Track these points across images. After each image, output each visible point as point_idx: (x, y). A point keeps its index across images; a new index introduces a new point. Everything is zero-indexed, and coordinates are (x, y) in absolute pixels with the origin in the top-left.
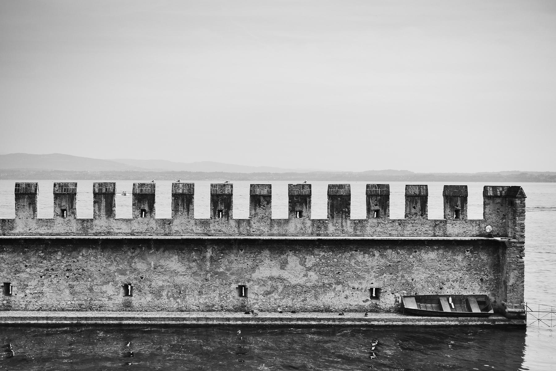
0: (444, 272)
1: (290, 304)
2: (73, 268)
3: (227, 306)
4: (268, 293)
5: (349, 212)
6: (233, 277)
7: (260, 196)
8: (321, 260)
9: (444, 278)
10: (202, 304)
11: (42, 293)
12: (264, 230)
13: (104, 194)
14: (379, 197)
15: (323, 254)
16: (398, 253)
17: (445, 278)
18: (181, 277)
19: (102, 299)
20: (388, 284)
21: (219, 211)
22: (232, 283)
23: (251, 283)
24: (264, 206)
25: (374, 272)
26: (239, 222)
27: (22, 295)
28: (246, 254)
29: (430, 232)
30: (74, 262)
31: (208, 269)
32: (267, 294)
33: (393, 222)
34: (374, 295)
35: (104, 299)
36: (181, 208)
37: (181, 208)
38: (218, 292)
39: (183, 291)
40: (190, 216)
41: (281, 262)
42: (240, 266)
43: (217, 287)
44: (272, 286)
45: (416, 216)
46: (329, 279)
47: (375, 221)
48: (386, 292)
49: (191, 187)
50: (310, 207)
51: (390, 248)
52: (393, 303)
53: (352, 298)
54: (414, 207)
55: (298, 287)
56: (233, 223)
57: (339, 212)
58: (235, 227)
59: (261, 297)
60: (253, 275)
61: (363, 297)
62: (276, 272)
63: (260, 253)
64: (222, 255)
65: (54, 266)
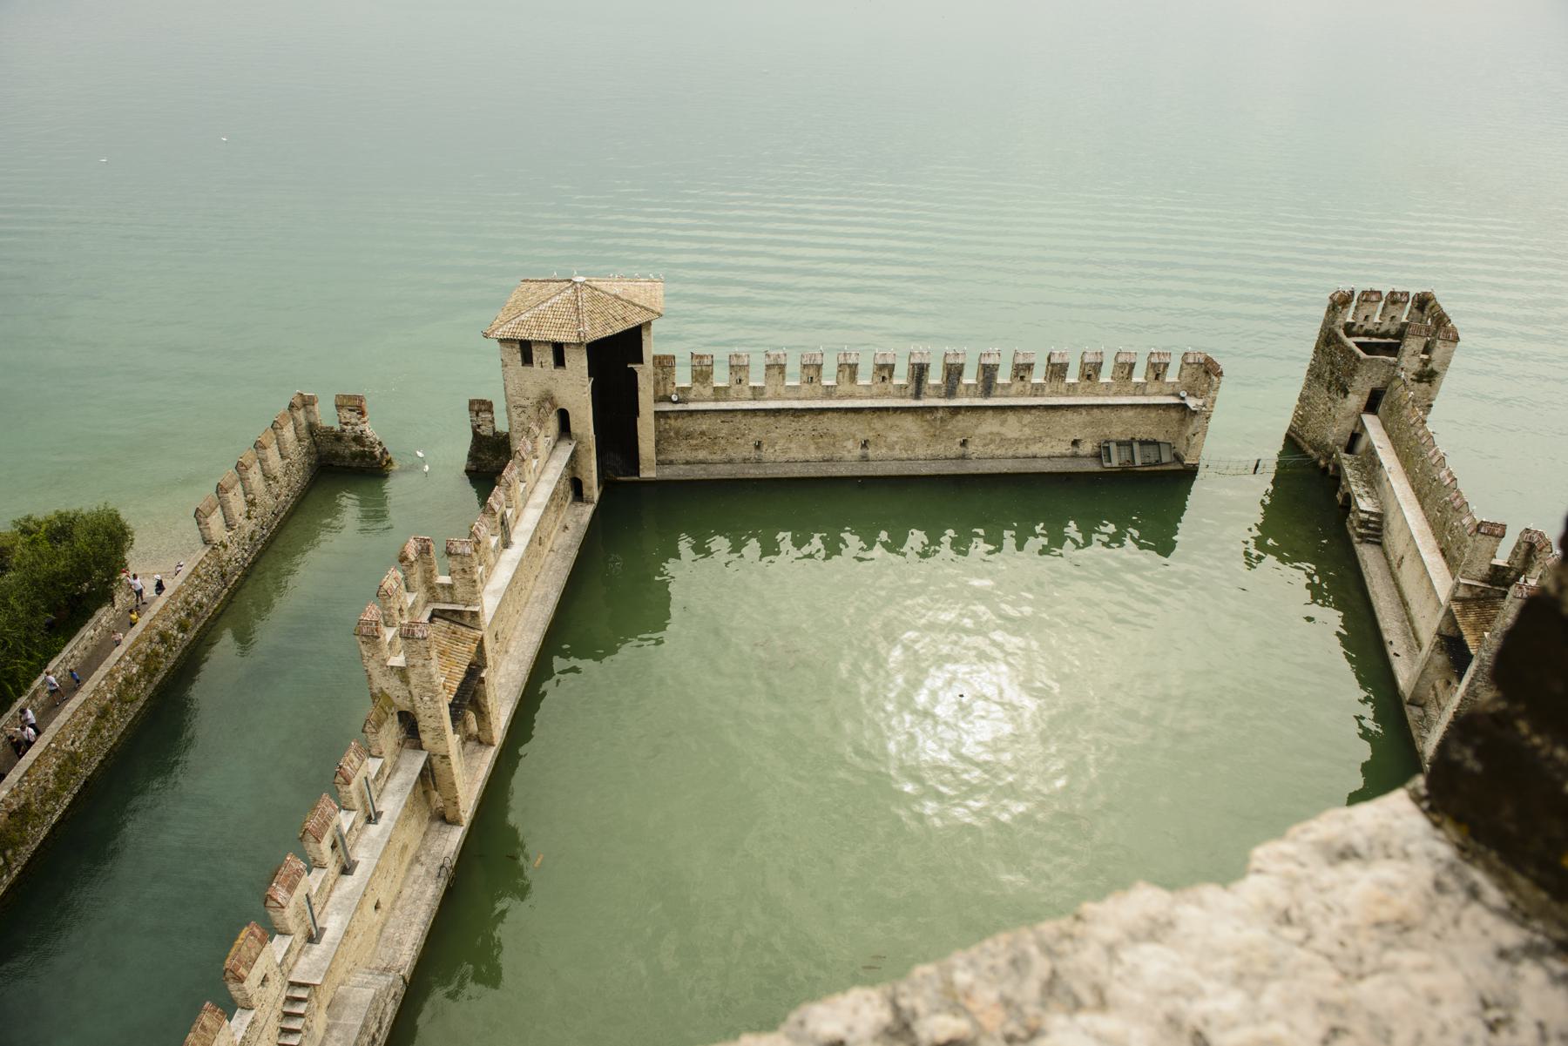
5: (1065, 377)
6: (958, 433)
11: (790, 449)
27: (772, 451)
42: (966, 424)
44: (991, 440)
59: (981, 448)
62: (996, 429)
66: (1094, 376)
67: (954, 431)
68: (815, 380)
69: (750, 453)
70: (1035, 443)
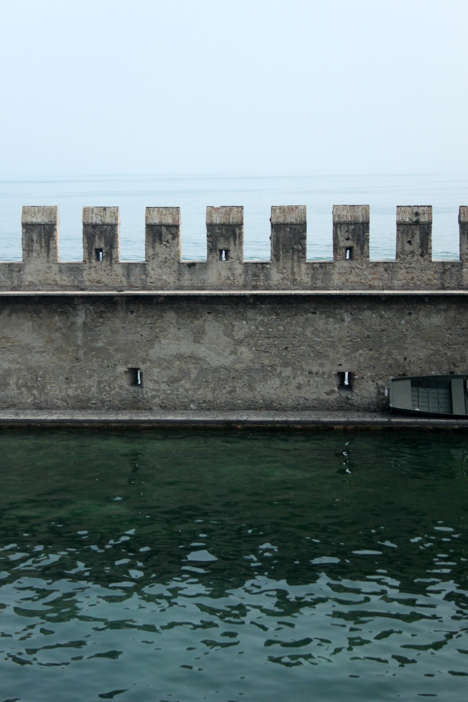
0: (455, 346)
1: (210, 396)
3: (110, 401)
4: (173, 381)
5: (304, 251)
6: (119, 356)
7: (161, 225)
8: (257, 328)
9: (456, 356)
10: (72, 397)
12: (169, 280)
14: (353, 227)
15: (262, 317)
16: (381, 317)
17: (458, 357)
18: (38, 355)
20: (365, 365)
21: (98, 251)
22: (117, 365)
23: (148, 364)
24: (167, 242)
25: (343, 347)
26: (129, 267)
28: (139, 319)
29: (435, 282)
31: (79, 342)
32: (173, 382)
33: (376, 266)
34: (346, 383)
36: (36, 246)
37: (36, 246)
38: (97, 379)
39: (41, 377)
40: (52, 258)
41: (195, 330)
42: (130, 337)
43: (95, 371)
44: (181, 370)
45: (413, 256)
46: (271, 358)
47: (345, 264)
48: (363, 378)
49: (52, 211)
50: (241, 243)
51: (369, 308)
52: (374, 395)
53: (308, 388)
54: (410, 242)
55: (222, 370)
56: (119, 270)
57: (287, 251)
58: (123, 275)
60: (151, 352)
61: (326, 387)
63: (161, 317)
64: (101, 320)
66: (357, 249)
67: (111, 349)
70: (264, 379)
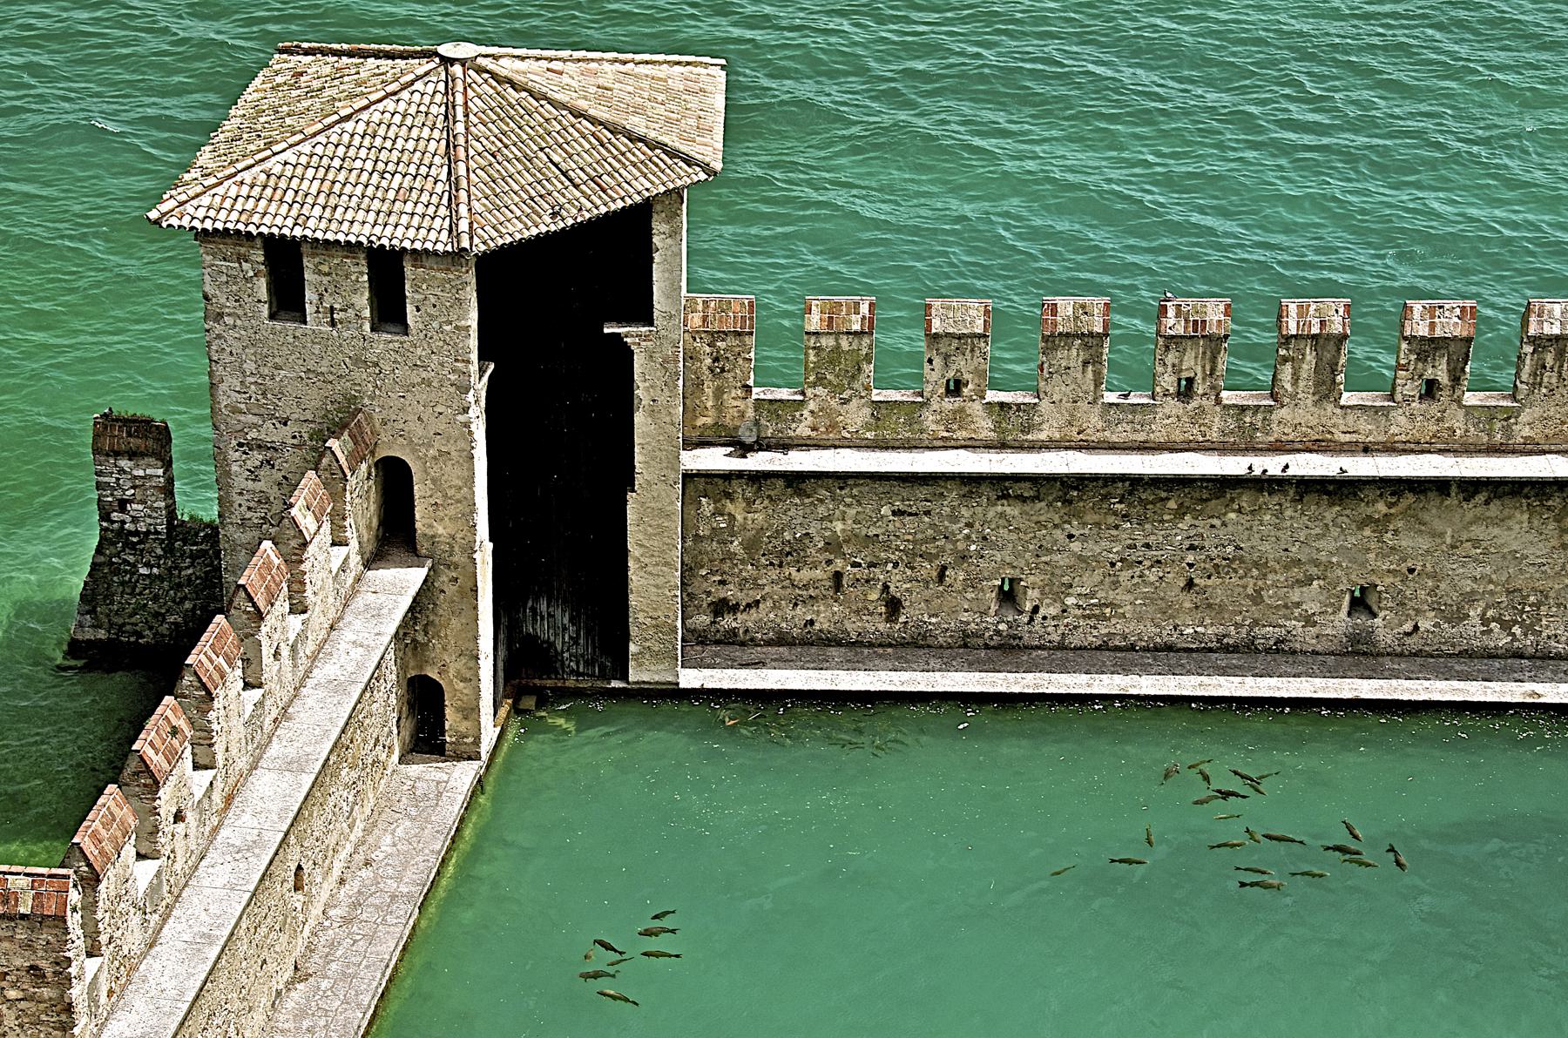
2: (1206, 544)
13: (1314, 337)
19: (1287, 624)
30: (1213, 526)
35: (1294, 622)
65: (1153, 537)
68: (1200, 388)
69: (984, 613)
